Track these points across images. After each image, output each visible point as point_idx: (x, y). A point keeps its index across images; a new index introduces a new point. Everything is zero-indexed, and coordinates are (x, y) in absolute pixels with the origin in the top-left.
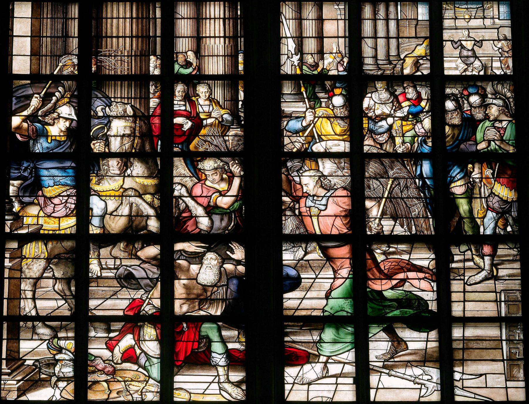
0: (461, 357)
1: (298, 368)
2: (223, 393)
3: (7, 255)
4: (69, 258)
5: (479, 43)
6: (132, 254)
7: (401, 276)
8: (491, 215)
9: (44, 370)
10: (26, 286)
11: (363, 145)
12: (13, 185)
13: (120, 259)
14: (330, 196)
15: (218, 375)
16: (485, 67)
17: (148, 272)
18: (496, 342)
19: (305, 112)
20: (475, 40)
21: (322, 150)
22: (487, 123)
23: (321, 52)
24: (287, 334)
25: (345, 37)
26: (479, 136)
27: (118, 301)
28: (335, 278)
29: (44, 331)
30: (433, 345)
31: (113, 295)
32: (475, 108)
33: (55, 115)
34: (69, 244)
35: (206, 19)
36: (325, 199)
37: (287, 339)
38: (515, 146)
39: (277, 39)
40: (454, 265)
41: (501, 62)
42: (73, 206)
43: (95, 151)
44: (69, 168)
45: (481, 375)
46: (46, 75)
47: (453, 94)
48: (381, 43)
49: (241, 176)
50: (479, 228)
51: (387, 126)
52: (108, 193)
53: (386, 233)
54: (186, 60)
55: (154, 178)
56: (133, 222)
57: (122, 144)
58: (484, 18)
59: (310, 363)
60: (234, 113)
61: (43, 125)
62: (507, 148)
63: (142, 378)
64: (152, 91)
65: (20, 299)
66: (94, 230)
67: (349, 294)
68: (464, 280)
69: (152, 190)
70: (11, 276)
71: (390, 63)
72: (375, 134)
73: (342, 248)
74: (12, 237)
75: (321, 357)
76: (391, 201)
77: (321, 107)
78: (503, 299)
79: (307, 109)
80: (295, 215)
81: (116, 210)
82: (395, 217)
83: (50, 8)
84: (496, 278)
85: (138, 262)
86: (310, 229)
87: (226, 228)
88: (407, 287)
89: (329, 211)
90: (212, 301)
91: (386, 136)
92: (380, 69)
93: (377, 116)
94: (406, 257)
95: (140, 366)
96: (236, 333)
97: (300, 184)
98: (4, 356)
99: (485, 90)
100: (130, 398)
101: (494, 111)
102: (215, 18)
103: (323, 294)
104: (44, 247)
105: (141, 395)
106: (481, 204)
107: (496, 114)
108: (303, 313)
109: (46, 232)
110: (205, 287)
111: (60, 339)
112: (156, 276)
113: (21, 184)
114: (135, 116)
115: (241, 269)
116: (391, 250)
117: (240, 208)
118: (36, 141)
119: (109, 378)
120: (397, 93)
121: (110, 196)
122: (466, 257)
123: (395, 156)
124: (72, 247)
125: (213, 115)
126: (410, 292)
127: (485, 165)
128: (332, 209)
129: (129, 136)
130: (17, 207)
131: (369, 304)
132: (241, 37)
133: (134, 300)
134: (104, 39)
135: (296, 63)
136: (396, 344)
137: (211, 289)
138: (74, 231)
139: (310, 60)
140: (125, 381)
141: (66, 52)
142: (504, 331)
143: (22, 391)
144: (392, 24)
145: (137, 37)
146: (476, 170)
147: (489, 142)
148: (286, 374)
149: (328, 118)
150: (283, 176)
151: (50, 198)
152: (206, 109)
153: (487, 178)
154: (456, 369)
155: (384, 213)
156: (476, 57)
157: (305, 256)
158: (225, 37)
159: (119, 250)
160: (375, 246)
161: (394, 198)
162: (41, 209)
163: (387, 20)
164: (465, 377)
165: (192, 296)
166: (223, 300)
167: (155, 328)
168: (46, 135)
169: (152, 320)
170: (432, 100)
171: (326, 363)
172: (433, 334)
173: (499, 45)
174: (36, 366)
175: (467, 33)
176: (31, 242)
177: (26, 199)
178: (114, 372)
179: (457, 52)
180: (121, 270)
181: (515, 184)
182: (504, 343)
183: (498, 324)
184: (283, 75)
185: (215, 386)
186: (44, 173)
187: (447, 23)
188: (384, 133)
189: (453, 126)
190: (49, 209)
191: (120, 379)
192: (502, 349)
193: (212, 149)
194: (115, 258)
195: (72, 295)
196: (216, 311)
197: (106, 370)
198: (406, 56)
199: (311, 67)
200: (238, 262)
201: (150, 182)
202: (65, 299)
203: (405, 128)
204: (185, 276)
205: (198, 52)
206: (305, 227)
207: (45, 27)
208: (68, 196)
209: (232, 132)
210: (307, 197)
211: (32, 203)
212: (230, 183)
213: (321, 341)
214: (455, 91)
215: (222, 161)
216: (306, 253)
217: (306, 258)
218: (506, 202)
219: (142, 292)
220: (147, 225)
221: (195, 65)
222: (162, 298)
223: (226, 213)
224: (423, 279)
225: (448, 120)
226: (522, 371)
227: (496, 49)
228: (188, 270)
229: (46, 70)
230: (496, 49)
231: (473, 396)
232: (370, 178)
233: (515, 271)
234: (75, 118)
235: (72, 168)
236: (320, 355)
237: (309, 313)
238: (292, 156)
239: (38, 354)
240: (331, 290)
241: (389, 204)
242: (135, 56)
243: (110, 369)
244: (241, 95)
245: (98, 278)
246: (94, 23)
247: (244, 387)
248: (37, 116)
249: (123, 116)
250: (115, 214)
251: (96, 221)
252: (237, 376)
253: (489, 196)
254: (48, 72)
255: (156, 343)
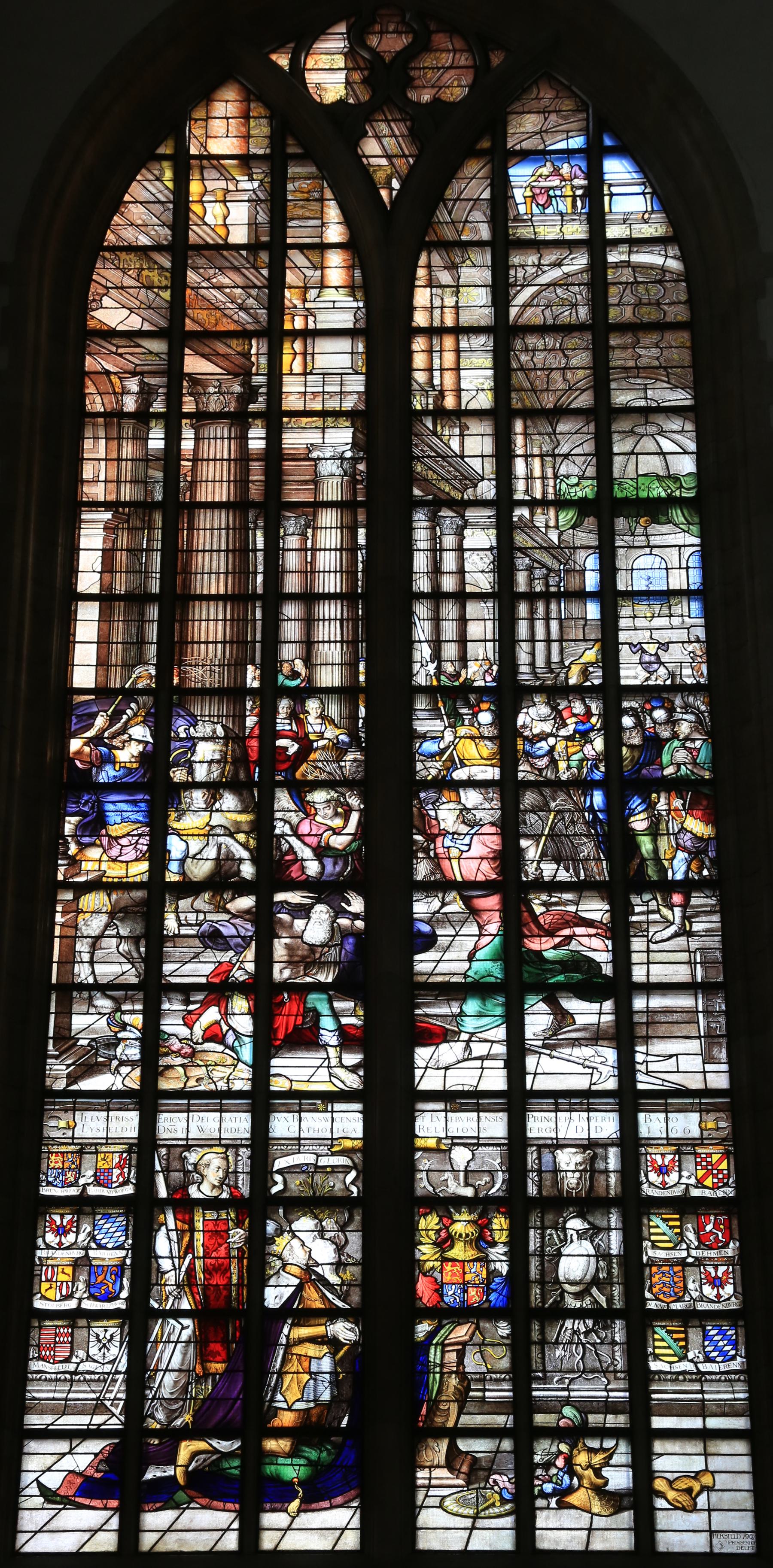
0: (645, 1033)
1: (433, 1048)
2: (333, 1079)
3: (59, 908)
4: (138, 912)
5: (665, 646)
6: (219, 907)
7: (567, 932)
8: (681, 855)
9: (101, 1051)
10: (82, 947)
11: (517, 771)
12: (69, 823)
13: (205, 913)
14: (475, 834)
15: (328, 1058)
16: (672, 675)
17: (240, 929)
18: (690, 1015)
19: (443, 732)
20: (658, 642)
21: (465, 777)
22: (676, 743)
23: (463, 660)
24: (418, 1006)
25: (494, 641)
26: (665, 758)
27: (200, 965)
28: (480, 935)
29: (104, 1004)
30: (608, 1018)
31: (194, 958)
32: (660, 724)
33: (126, 737)
34: (138, 894)
35: (319, 620)
36: (468, 838)
37: (418, 1012)
38: (713, 770)
39: (409, 644)
40: (634, 918)
41: (693, 669)
42: (145, 848)
43: (175, 780)
44: (141, 801)
45: (671, 1056)
46: (115, 689)
47: (631, 708)
48: (540, 647)
49: (360, 810)
50: (666, 871)
51: (547, 748)
52: (190, 832)
53: (546, 879)
54: (292, 670)
55: (248, 813)
56: (221, 867)
57: (209, 772)
58: (671, 616)
59: (448, 1041)
60: (353, 733)
61: (110, 749)
62: (702, 773)
63: (229, 1061)
64: (248, 707)
65: (74, 962)
66: (172, 876)
67: (499, 955)
68: (647, 936)
69: (246, 828)
70: (64, 934)
71: (551, 671)
72: (533, 757)
73: (491, 898)
74: (66, 885)
75: (463, 1034)
76: (553, 840)
77: (463, 725)
78: (698, 960)
79: (446, 728)
80: (429, 857)
81: (200, 852)
82: (557, 859)
83: (122, 609)
84: (690, 934)
85: (226, 917)
86: (449, 874)
87: (340, 874)
88: (574, 946)
89: (474, 852)
90: (321, 965)
91: (545, 760)
92: (539, 679)
93: (534, 736)
94: (572, 908)
95: (227, 1047)
96: (352, 1004)
97: (436, 819)
98: (51, 1034)
99: (673, 703)
100: (212, 1087)
101: (684, 729)
102: (330, 620)
103: (465, 955)
104: (106, 898)
105: (228, 1083)
106: (669, 842)
107: (687, 731)
108: (440, 979)
109: (110, 880)
110: (312, 947)
111: (123, 1012)
112: (250, 934)
113: (80, 821)
114: (226, 738)
115: (360, 924)
116: (553, 900)
117: (359, 849)
118: (100, 768)
119: (186, 1061)
120: (560, 708)
121: (193, 835)
122: (651, 908)
123: (557, 785)
124: (142, 898)
125: (326, 735)
126: (578, 952)
127: (673, 794)
128: (478, 849)
129: (218, 762)
130: (73, 849)
131: (526, 968)
132: (362, 642)
133: (220, 963)
134: (190, 646)
135: (432, 673)
136: (559, 1017)
137: (320, 949)
138: (145, 878)
139: (449, 668)
140: (206, 1066)
141: (141, 661)
142: (700, 1001)
143: (73, 1078)
144: (554, 625)
145: (231, 642)
146: (663, 800)
147: (678, 765)
148: (416, 1056)
149: (472, 738)
150: (415, 809)
151: (116, 838)
152: (317, 728)
153: (676, 810)
154: (638, 1048)
155: (543, 855)
156: (661, 663)
157: (441, 908)
158: (342, 642)
159: (202, 902)
160: (532, 896)
161: (557, 835)
162: (105, 851)
163: (547, 619)
164: (650, 1058)
165: (296, 959)
166: (336, 963)
167: (247, 999)
168: (113, 761)
169: (242, 988)
170: (605, 716)
171: (468, 1042)
172: (608, 1005)
173: (690, 648)
174: (92, 1047)
175: (648, 633)
176: (90, 892)
177: (86, 840)
178: (193, 1054)
179: (636, 658)
180: (205, 926)
181: (713, 818)
182: (701, 1015)
183: (692, 992)
184: (415, 687)
185: (324, 1072)
186: (109, 807)
187: (623, 623)
188: (543, 756)
189: (632, 747)
190: (114, 852)
191: (201, 1063)
192: (698, 1023)
193: (324, 776)
194: (198, 912)
195: (141, 957)
196: (326, 977)
197: (183, 1052)
198: (571, 663)
199: (451, 677)
200: (356, 916)
201: (244, 818)
202: (132, 963)
203: (570, 750)
204: (287, 932)
205: (308, 661)
206: (442, 872)
207: (115, 631)
208: (140, 835)
209: (350, 757)
210: (445, 835)
211: (92, 845)
212: (347, 818)
213: (462, 1014)
214: (634, 704)
215: (336, 792)
216: (444, 904)
217: (443, 911)
218: (700, 839)
219: (231, 953)
220: (239, 871)
221: (303, 674)
222: (257, 961)
223: (341, 856)
224: (595, 935)
225: (625, 740)
226: (724, 1051)
227: (686, 653)
228: (291, 926)
229: (115, 683)
230: (686, 653)
231: (660, 1082)
232: (526, 811)
233: (713, 925)
234: (151, 740)
235: (145, 801)
236: (461, 1031)
237: (447, 978)
238: (426, 785)
239: (95, 1031)
240: (476, 949)
241: (550, 844)
242: (228, 665)
243: (188, 1050)
244: (362, 712)
245: (175, 936)
246: (177, 626)
247: (361, 1073)
248: (103, 738)
249: (213, 738)
250: (198, 857)
251: (174, 866)
252: (352, 1059)
253: (679, 832)
254: (118, 686)
255: (248, 1017)
